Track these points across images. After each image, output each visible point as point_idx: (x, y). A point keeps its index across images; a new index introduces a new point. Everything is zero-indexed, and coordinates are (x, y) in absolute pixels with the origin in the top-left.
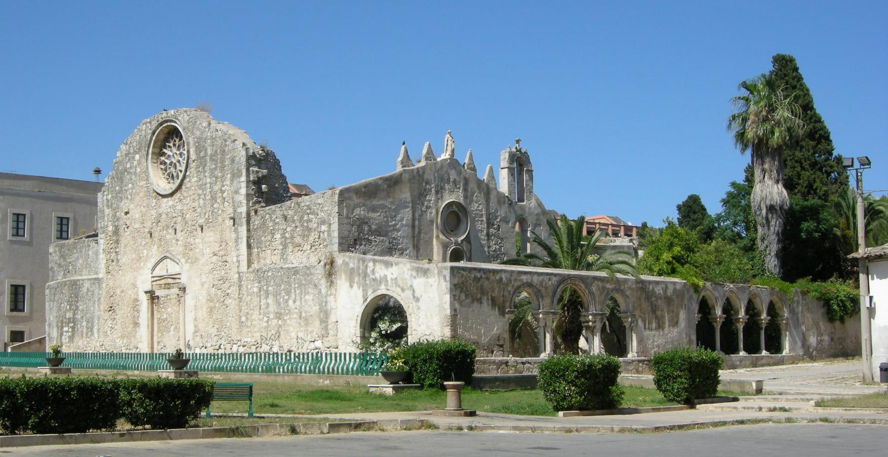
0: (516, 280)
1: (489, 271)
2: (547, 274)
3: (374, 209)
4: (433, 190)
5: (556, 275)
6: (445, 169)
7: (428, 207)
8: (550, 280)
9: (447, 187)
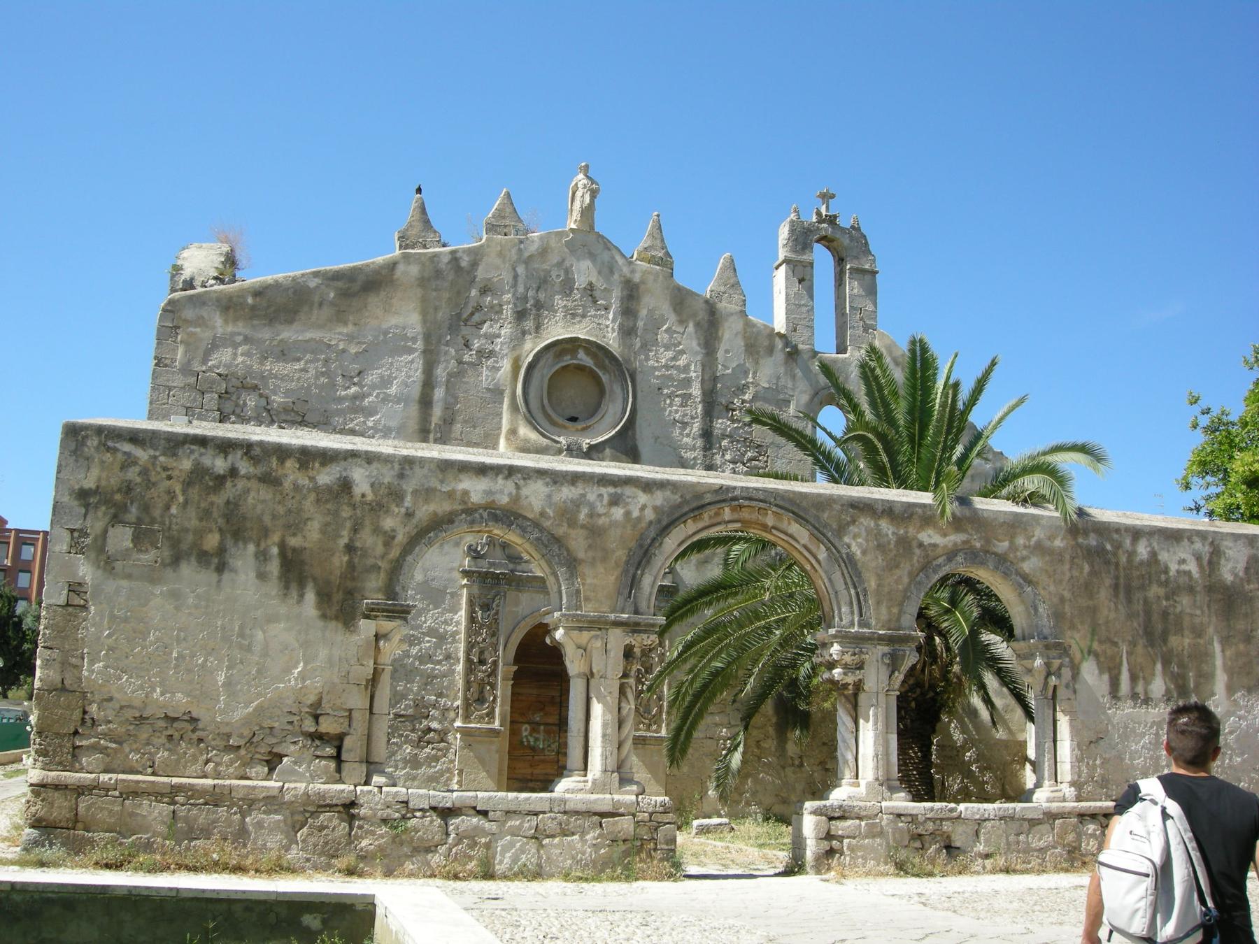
0: (427, 493)
1: (283, 452)
2: (604, 480)
3: (284, 353)
4: (508, 310)
5: (648, 486)
6: (554, 258)
7: (484, 354)
8: (615, 501)
9: (559, 301)
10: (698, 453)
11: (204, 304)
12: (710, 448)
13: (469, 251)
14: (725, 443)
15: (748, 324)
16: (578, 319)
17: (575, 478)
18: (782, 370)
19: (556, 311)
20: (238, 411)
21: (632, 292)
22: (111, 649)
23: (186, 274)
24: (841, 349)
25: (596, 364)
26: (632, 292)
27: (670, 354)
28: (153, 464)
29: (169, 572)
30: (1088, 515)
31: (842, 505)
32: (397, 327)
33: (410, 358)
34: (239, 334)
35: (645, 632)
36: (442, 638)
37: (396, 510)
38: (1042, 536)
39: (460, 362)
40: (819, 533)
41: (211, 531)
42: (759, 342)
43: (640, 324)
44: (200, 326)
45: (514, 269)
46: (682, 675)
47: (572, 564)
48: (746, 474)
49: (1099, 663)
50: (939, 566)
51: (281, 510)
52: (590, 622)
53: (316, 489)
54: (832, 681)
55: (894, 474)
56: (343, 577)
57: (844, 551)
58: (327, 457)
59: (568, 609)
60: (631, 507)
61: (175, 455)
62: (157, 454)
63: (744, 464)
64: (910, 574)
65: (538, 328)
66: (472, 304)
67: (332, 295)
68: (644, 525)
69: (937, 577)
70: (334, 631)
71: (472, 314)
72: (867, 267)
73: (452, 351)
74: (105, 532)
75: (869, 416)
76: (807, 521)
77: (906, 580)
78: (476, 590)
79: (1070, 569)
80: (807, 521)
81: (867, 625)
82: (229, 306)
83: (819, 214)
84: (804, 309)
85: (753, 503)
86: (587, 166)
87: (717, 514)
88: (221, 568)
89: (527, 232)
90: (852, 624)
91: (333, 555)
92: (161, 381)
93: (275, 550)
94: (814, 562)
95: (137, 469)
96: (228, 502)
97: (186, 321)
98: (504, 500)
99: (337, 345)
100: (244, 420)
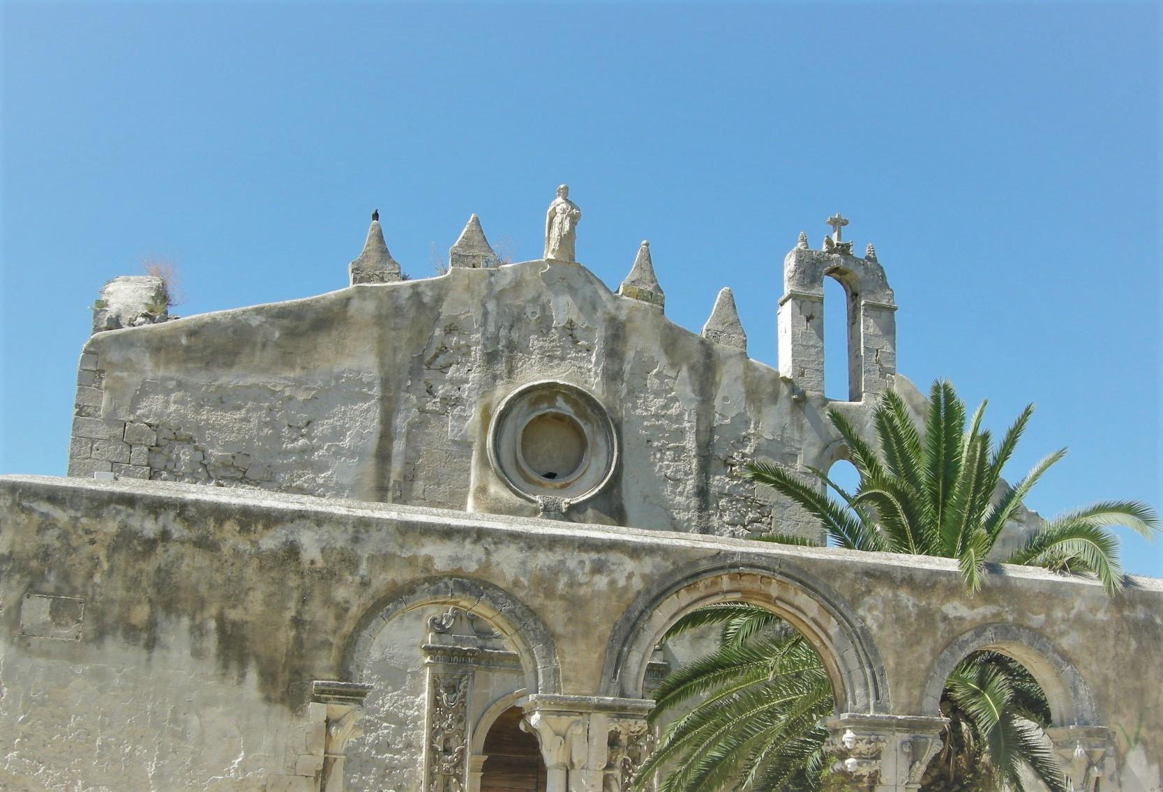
1: (220, 513)
2: (585, 545)
3: (222, 401)
4: (477, 352)
5: (636, 551)
6: (529, 293)
7: (450, 402)
8: (598, 568)
9: (535, 342)
10: (692, 514)
11: (132, 344)
12: (706, 509)
13: (433, 285)
14: (723, 502)
15: (749, 368)
16: (556, 362)
17: (553, 542)
18: (787, 420)
19: (532, 353)
20: (170, 466)
21: (617, 333)
22: (26, 736)
23: (112, 310)
24: (855, 396)
25: (576, 413)
26: (617, 333)
27: (660, 402)
28: (75, 527)
29: (92, 649)
30: (1135, 584)
31: (856, 573)
32: (351, 371)
33: (365, 406)
34: (172, 379)
35: (632, 717)
36: (402, 724)
37: (350, 578)
38: (1083, 608)
39: (422, 411)
40: (829, 604)
41: (139, 602)
42: (762, 388)
43: (627, 367)
44: (127, 369)
45: (484, 305)
46: (673, 766)
47: (549, 639)
48: (747, 537)
49: (1147, 752)
50: (966, 642)
51: (219, 578)
52: (570, 706)
53: (259, 554)
54: (844, 773)
55: (914, 537)
56: (290, 654)
57: (858, 625)
58: (271, 519)
59: (545, 691)
60: (616, 576)
61: (99, 516)
62: (79, 515)
63: (745, 527)
64: (933, 651)
65: (511, 372)
66: (436, 345)
67: (277, 334)
68: (631, 595)
69: (963, 655)
70: (280, 716)
71: (436, 356)
72: (884, 302)
73: (414, 398)
74: (20, 603)
75: (886, 472)
76: (816, 591)
77: (928, 658)
78: (440, 669)
79: (1115, 645)
80: (816, 591)
81: (885, 710)
82: (160, 347)
83: (829, 243)
84: (813, 351)
85: (755, 571)
86: (566, 188)
87: (714, 583)
88: (151, 644)
89: (499, 263)
90: (867, 708)
91: (277, 630)
92: (84, 432)
93: (212, 624)
94: (824, 637)
95: (56, 532)
96: (159, 570)
97: (111, 364)
98: (472, 567)
99: (282, 391)
100: (177, 477)
